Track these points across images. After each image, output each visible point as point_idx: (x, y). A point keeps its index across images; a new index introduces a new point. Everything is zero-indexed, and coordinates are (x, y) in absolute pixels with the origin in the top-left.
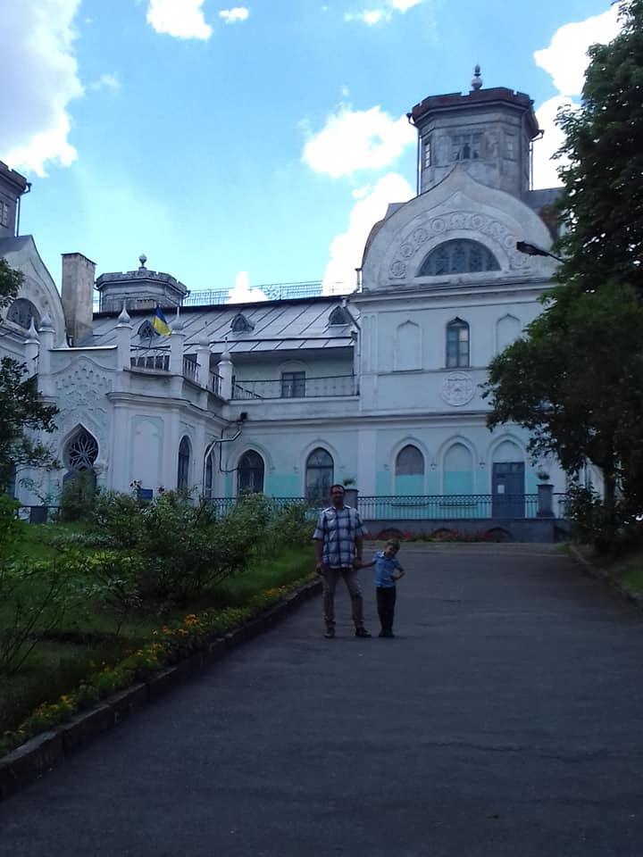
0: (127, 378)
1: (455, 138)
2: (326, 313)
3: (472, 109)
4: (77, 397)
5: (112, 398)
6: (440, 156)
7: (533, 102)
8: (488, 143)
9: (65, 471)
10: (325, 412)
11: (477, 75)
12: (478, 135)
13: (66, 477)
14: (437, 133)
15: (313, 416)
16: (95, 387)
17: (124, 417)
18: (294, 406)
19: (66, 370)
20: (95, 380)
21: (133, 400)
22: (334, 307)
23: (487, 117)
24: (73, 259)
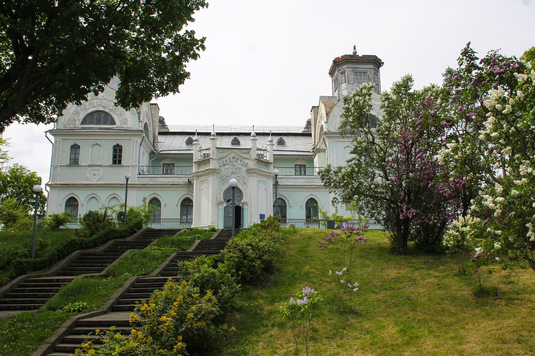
0: (255, 162)
1: (356, 73)
2: (276, 139)
3: (362, 62)
4: (231, 170)
5: (249, 171)
6: (350, 80)
7: (383, 63)
8: (369, 77)
9: (225, 205)
10: (313, 182)
11: (355, 49)
12: (365, 73)
13: (225, 208)
14: (348, 69)
15: (308, 184)
16: (240, 166)
17: (253, 181)
18: (299, 179)
19: (224, 157)
20: (239, 162)
21: (259, 173)
22: (280, 137)
23: (368, 66)
24: (154, 106)
